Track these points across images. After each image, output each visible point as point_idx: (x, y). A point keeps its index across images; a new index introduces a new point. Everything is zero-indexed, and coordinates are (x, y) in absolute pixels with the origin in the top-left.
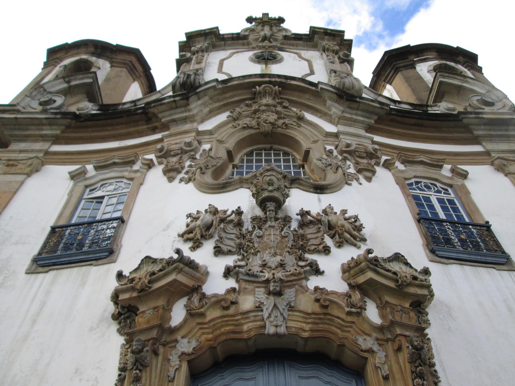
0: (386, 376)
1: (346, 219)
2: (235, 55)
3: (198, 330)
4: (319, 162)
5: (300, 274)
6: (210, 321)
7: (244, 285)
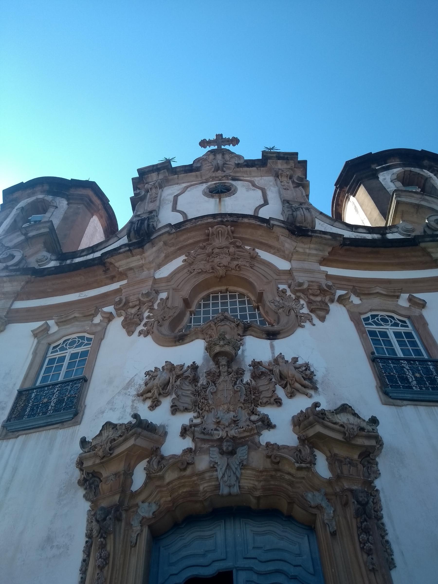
0: (333, 532)
1: (296, 368)
2: (189, 189)
3: (157, 494)
4: (272, 304)
5: (252, 429)
6: (169, 484)
7: (199, 445)
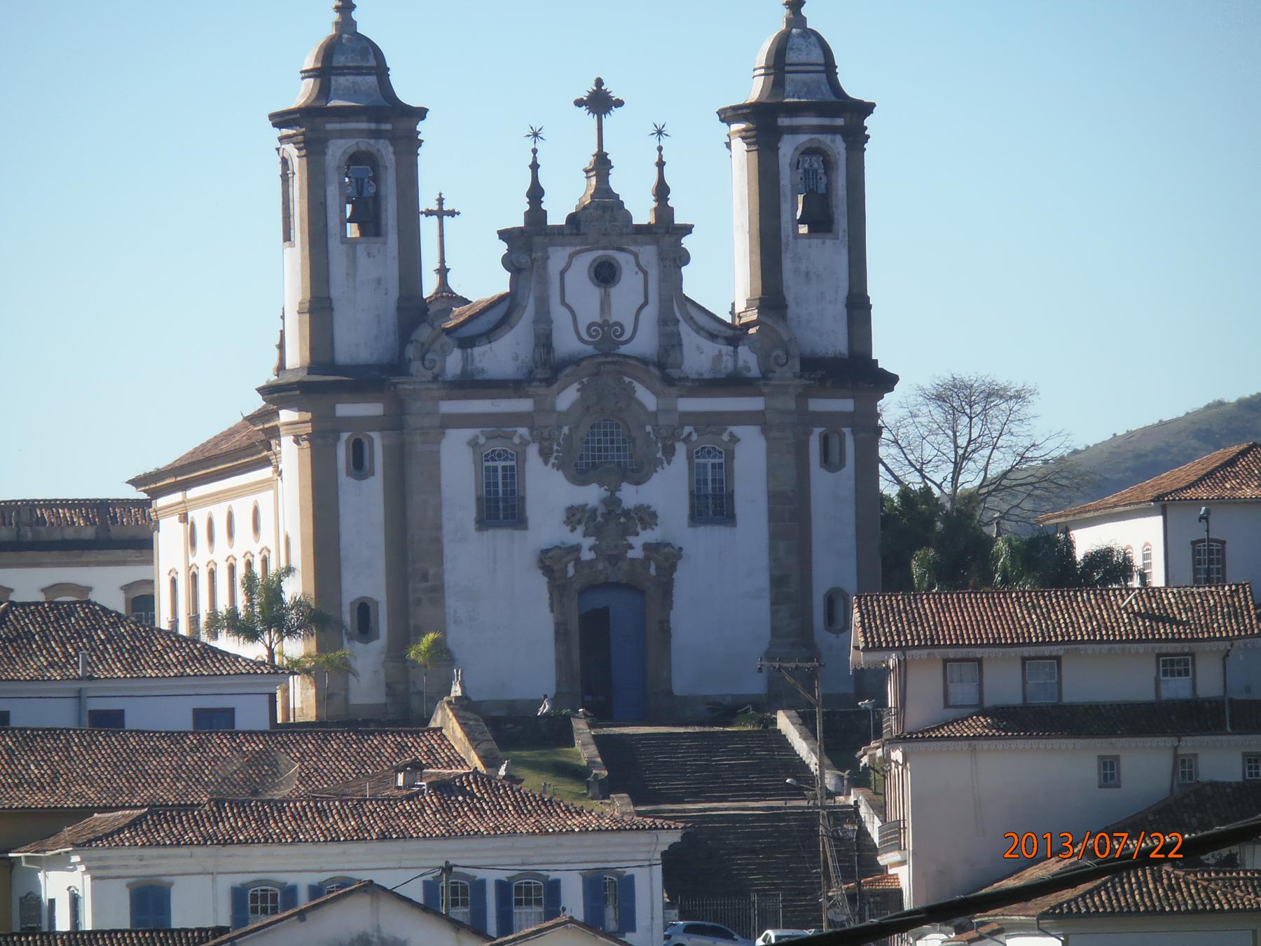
2: (574, 262)
